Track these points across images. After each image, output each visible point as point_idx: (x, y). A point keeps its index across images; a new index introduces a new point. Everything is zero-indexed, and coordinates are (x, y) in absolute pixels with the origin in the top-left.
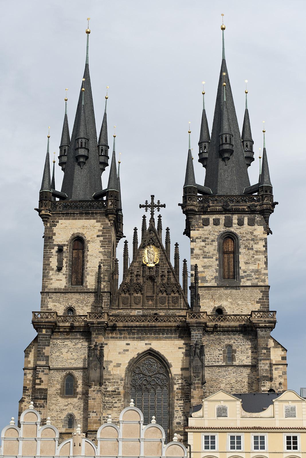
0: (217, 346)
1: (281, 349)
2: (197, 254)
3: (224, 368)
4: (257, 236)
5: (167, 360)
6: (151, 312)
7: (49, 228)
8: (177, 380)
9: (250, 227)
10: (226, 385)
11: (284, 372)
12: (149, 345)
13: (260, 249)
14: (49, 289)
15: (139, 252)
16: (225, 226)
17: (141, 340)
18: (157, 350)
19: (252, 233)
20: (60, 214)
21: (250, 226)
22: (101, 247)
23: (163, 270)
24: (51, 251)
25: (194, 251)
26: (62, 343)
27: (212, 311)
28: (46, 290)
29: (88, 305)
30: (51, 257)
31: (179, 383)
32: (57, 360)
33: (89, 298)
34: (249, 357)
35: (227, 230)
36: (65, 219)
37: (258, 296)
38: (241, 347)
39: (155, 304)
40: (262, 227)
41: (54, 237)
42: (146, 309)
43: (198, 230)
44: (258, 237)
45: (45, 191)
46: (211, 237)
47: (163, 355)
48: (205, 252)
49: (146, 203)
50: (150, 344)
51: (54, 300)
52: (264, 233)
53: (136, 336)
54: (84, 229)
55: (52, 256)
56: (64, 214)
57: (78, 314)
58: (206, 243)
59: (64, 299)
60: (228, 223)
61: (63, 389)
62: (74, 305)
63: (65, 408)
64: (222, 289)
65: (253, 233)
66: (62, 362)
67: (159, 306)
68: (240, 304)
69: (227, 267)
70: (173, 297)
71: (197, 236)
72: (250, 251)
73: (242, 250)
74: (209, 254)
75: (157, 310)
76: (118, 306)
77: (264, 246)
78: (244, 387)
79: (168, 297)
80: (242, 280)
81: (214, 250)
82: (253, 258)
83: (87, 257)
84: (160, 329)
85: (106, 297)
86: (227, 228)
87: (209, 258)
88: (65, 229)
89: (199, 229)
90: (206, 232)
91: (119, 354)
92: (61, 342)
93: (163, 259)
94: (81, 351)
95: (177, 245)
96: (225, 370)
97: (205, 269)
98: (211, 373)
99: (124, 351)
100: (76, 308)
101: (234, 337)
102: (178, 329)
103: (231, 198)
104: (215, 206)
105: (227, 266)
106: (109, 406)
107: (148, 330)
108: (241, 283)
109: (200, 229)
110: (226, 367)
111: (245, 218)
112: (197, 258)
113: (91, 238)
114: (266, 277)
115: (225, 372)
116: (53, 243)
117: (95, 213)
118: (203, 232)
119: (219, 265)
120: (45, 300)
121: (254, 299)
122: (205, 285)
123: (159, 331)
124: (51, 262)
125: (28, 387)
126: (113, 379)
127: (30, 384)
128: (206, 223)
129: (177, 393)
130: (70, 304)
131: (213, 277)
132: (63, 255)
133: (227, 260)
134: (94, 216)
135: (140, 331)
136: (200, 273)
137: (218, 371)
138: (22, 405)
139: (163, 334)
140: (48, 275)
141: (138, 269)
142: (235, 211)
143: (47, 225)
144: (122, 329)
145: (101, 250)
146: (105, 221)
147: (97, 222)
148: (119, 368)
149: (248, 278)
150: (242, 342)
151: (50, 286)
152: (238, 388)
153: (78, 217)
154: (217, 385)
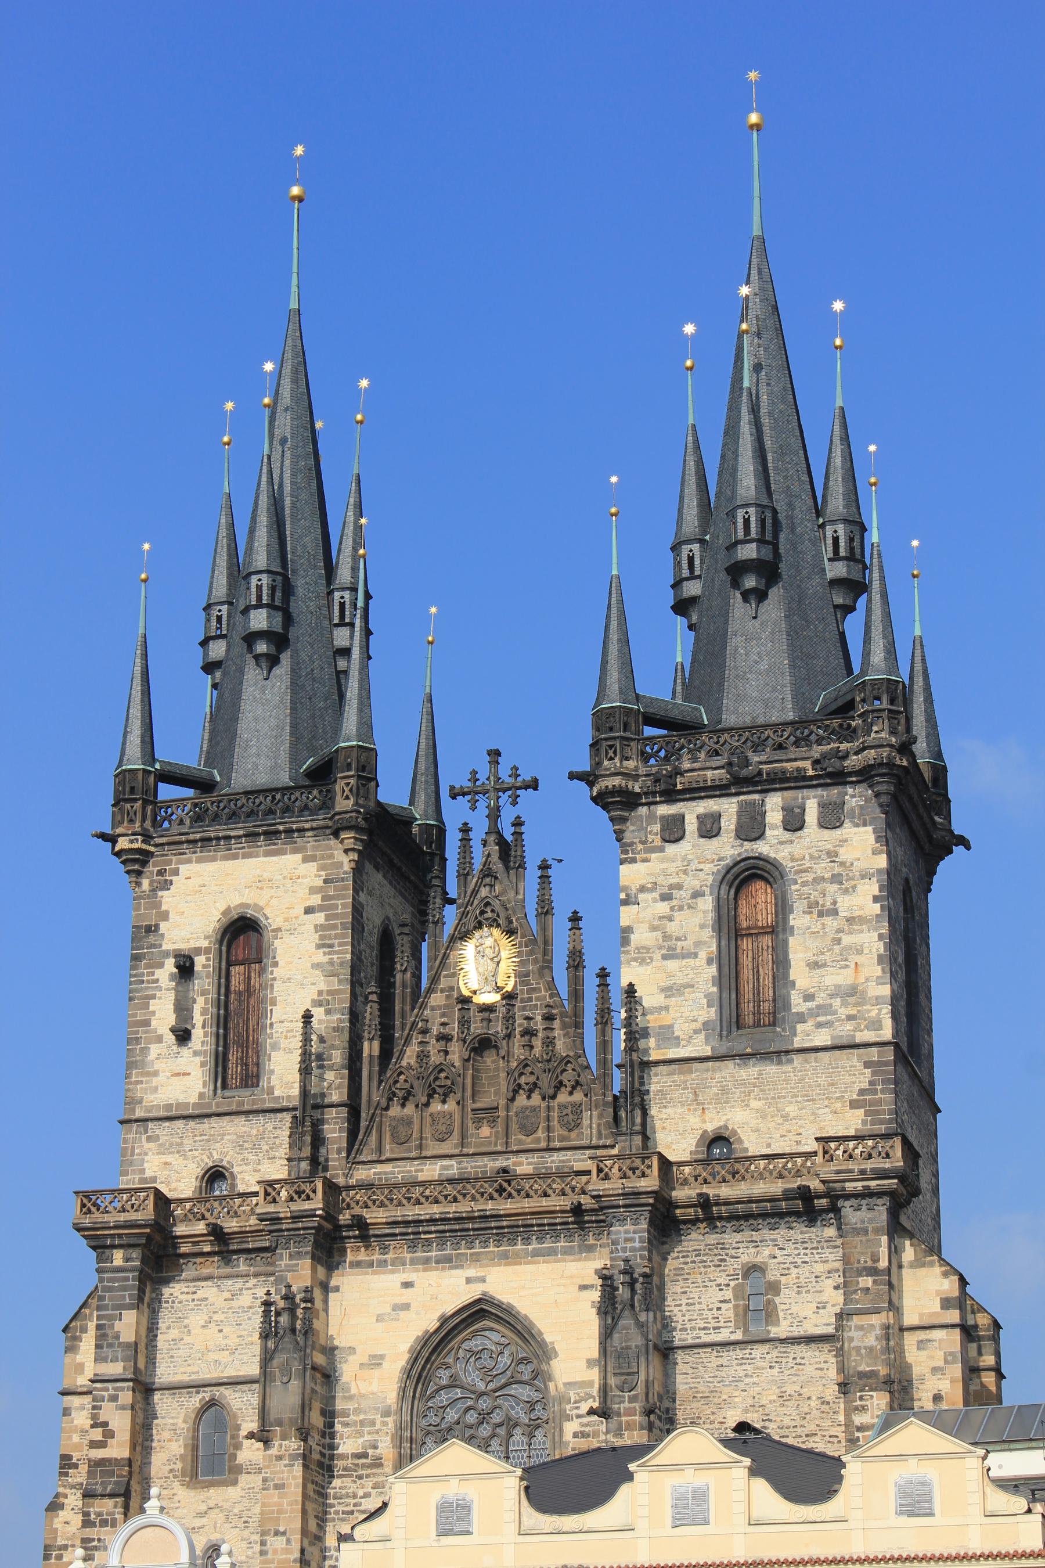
0: (712, 1272)
1: (937, 1270)
2: (643, 948)
3: (739, 1353)
4: (852, 864)
5: (541, 1333)
6: (486, 1166)
8: (575, 1402)
11: (951, 1354)
13: (861, 908)
14: (149, 1109)
15: (445, 957)
16: (738, 836)
17: (451, 1268)
18: (505, 1301)
19: (832, 855)
20: (181, 843)
21: (826, 832)
22: (319, 947)
23: (527, 1013)
24: (153, 974)
25: (632, 936)
26: (188, 1293)
27: (693, 1148)
28: (139, 1113)
29: (277, 1154)
30: (154, 997)
32: (172, 1357)
33: (279, 1131)
34: (824, 1308)
35: (746, 851)
36: (199, 861)
37: (854, 1083)
38: (796, 1270)
39: (500, 1135)
40: (870, 829)
41: (163, 926)
42: (468, 1155)
44: (854, 868)
45: (130, 770)
46: (692, 883)
47: (526, 1316)
49: (474, 776)
50: (483, 1280)
51: (161, 1145)
52: (875, 852)
53: (434, 1254)
54: (261, 888)
55: (158, 994)
56: (195, 841)
57: (241, 1188)
58: (674, 902)
59: (197, 1138)
60: (752, 827)
61: (193, 1455)
62: (228, 1158)
63: (198, 1522)
64: (730, 1064)
65: (836, 855)
66: (190, 1362)
67: (519, 1140)
68: (792, 1115)
69: (751, 986)
71: (643, 882)
72: (828, 920)
73: (798, 920)
74: (683, 943)
75: (506, 1156)
76: (380, 1149)
77: (876, 899)
78: (808, 1416)
79: (548, 1107)
80: (799, 1027)
81: (702, 927)
82: (839, 944)
83: (272, 985)
84: (516, 1223)
85: (336, 1123)
86: (747, 845)
87: (684, 956)
89: (648, 855)
91: (377, 1320)
92: (186, 1290)
94: (250, 1319)
95: (575, 918)
96: (743, 1358)
98: (691, 1371)
99: (394, 1310)
100: (235, 1170)
101: (772, 1237)
103: (756, 735)
104: (700, 769)
105: (751, 982)
106: (346, 1509)
107: (474, 1230)
108: (796, 1039)
109: (653, 855)
110: (743, 1346)
111: (808, 802)
112: (643, 962)
113: (286, 920)
114: (884, 1011)
115: (741, 1364)
116: (160, 946)
117: (299, 830)
118: (664, 866)
119: (719, 981)
120: (133, 1148)
121: (843, 1092)
122: (672, 1053)
123: (510, 1230)
124: (153, 1013)
125: (76, 1456)
126: (357, 1411)
128: (673, 831)
130: (216, 1157)
131: (698, 1025)
132: (194, 985)
133: (750, 959)
134: (295, 842)
135: (448, 1234)
136: (652, 1013)
138: (56, 1520)
139: (527, 1241)
140: (143, 1061)
141: (443, 1015)
142: (772, 781)
143: (138, 884)
144: (387, 1231)
145: (320, 957)
146: (332, 856)
147: (305, 860)
148: (377, 1372)
149: (819, 1019)
150: (799, 1254)
151: (152, 1097)
152: (787, 1421)
153: (244, 848)
154: (713, 1413)
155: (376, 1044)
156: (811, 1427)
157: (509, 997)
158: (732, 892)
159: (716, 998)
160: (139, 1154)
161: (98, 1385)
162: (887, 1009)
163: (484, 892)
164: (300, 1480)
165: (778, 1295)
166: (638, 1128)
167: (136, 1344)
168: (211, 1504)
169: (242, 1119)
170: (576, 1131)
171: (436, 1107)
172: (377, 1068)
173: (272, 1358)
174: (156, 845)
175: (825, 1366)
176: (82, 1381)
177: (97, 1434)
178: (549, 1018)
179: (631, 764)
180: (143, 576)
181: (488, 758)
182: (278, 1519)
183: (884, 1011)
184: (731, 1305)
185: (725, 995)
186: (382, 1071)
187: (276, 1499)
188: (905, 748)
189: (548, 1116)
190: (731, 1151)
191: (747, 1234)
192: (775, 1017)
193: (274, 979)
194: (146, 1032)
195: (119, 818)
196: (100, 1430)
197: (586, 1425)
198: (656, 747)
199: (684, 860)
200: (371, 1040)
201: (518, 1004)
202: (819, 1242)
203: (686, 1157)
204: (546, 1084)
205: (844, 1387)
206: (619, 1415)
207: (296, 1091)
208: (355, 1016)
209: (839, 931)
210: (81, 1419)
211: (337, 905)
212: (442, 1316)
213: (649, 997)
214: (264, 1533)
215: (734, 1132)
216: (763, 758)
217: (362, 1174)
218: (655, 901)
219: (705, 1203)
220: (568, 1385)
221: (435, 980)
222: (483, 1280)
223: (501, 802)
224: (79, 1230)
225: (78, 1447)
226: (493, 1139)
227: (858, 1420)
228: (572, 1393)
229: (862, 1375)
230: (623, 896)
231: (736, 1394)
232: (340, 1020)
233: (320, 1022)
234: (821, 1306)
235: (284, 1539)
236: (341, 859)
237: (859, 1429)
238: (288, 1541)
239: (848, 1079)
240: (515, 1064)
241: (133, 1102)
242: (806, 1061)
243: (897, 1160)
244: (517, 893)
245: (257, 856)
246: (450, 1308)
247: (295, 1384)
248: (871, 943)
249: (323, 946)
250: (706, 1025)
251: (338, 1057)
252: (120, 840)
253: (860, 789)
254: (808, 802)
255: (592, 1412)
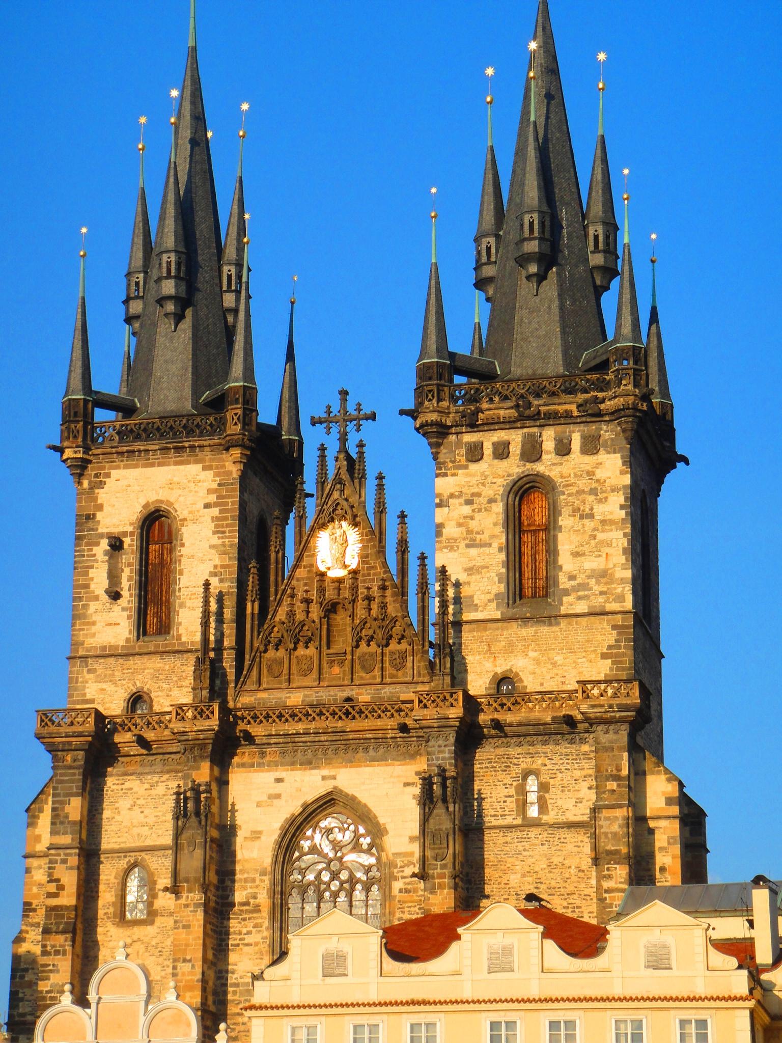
0: (501, 775)
1: (663, 777)
2: (452, 539)
3: (519, 833)
5: (376, 817)
6: (336, 695)
7: (88, 493)
8: (401, 867)
9: (588, 459)
10: (524, 876)
12: (333, 781)
13: (611, 513)
14: (88, 650)
15: (307, 542)
17: (312, 769)
19: (590, 474)
22: (214, 533)
23: (367, 585)
24: (91, 550)
25: (444, 531)
30: (92, 567)
31: (404, 874)
33: (185, 668)
34: (581, 802)
36: (126, 467)
38: (561, 775)
40: (618, 455)
41: (99, 516)
43: (454, 475)
44: (606, 484)
45: (74, 399)
46: (488, 492)
47: (365, 805)
48: (472, 531)
50: (334, 778)
51: (98, 676)
52: (622, 473)
54: (172, 489)
56: (122, 453)
58: (475, 506)
60: (532, 452)
62: (148, 686)
64: (514, 625)
68: (559, 662)
70: (392, 653)
71: (452, 491)
72: (586, 521)
73: (565, 521)
79: (382, 653)
80: (565, 599)
81: (495, 524)
83: (180, 561)
86: (529, 465)
88: (126, 492)
89: (456, 471)
90: (476, 479)
91: (257, 806)
92: (117, 782)
93: (367, 557)
94: (164, 803)
95: (403, 516)
97: (471, 575)
100: (153, 695)
102: (401, 735)
104: (495, 409)
109: (460, 471)
110: (522, 828)
111: (573, 435)
112: (451, 549)
113: (190, 513)
114: (627, 589)
116: (97, 529)
117: (200, 446)
118: (468, 479)
119: (507, 564)
124: (92, 579)
125: (35, 903)
127: (39, 894)
128: (475, 454)
129: (399, 901)
130: (138, 685)
131: (491, 596)
137: (502, 840)
141: (305, 585)
143: (80, 483)
144: (265, 741)
145: (215, 540)
147: (204, 469)
148: (257, 843)
149: (580, 593)
152: (553, 884)
155: (256, 604)
156: (571, 888)
157: (354, 573)
158: (517, 499)
159: (505, 576)
160: (82, 682)
161: (52, 852)
162: (628, 589)
163: (336, 495)
164: (202, 922)
165: (548, 792)
166: (448, 671)
167: (81, 822)
168: (135, 938)
169: (157, 658)
170: (402, 671)
171: (301, 651)
172: (256, 622)
173: (181, 833)
174: (94, 455)
175: (581, 844)
176: (41, 847)
177: (52, 888)
178: (383, 588)
179: (445, 404)
180: (82, 253)
181: (339, 397)
182: (186, 950)
183: (627, 589)
184: (513, 799)
185: (511, 574)
186: (261, 625)
187: (184, 936)
188: (646, 397)
189: (382, 660)
190: (514, 687)
191: (525, 748)
192: (547, 592)
193: (182, 556)
194: (86, 593)
195: (66, 434)
196: (54, 884)
197: (408, 884)
198: (463, 392)
199: (482, 475)
200: (253, 602)
201: (360, 578)
202: (577, 755)
203: (483, 692)
204: (380, 636)
205: (596, 861)
206: (433, 878)
207: (198, 637)
208: (241, 584)
209: (595, 529)
210: (40, 876)
211: (228, 503)
212: (304, 803)
213: (455, 573)
214: (175, 960)
215: (517, 675)
216: (541, 402)
217: (246, 699)
218: (461, 505)
219: (497, 725)
220: (396, 854)
221: (299, 559)
222: (334, 778)
223: (348, 429)
224: (39, 739)
225: (36, 896)
226: (341, 675)
227: (606, 884)
228: (398, 861)
229: (609, 853)
230: (437, 501)
231: (517, 863)
232: (230, 587)
233: (215, 588)
234: (579, 801)
235: (190, 965)
236: (231, 468)
237: (606, 891)
238: (193, 966)
239: (600, 638)
240: (358, 621)
241: (76, 644)
242: (569, 624)
243: (635, 698)
244: (360, 497)
245: (169, 465)
246: (310, 797)
247: (199, 853)
248: (619, 539)
249: (218, 532)
250: (497, 596)
251: (229, 613)
252: (67, 451)
253: (611, 426)
254: (573, 435)
255: (414, 875)
